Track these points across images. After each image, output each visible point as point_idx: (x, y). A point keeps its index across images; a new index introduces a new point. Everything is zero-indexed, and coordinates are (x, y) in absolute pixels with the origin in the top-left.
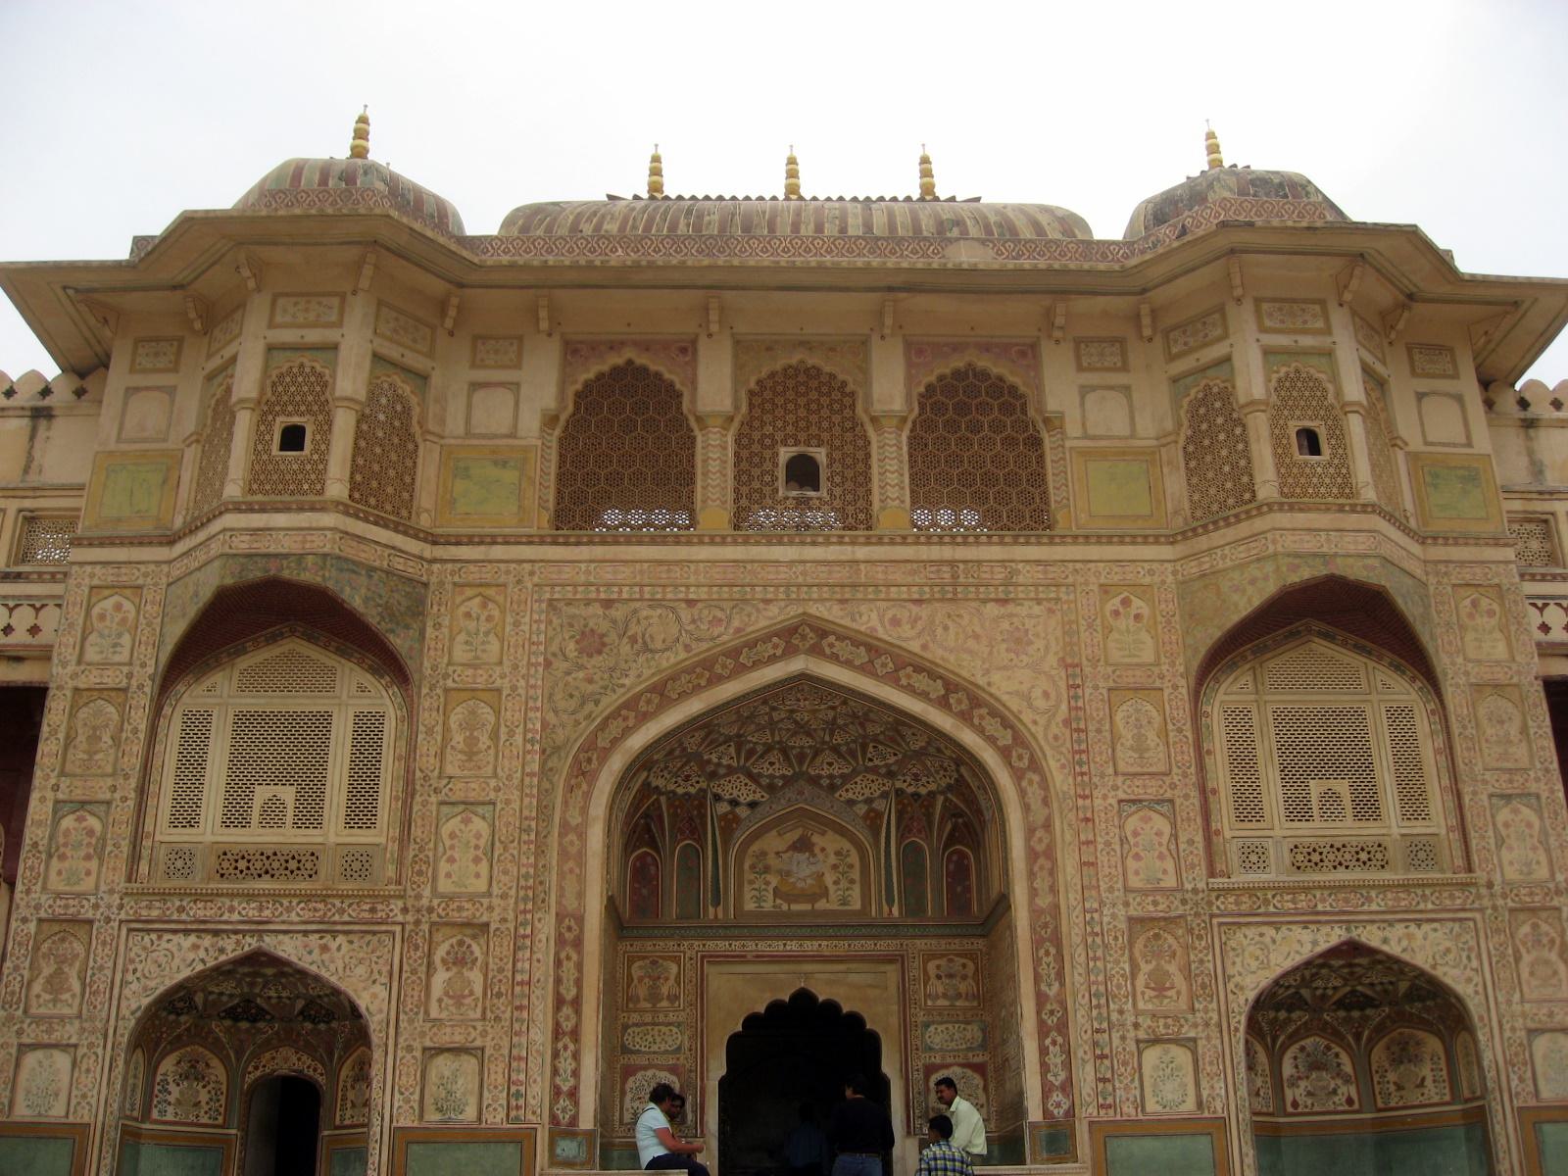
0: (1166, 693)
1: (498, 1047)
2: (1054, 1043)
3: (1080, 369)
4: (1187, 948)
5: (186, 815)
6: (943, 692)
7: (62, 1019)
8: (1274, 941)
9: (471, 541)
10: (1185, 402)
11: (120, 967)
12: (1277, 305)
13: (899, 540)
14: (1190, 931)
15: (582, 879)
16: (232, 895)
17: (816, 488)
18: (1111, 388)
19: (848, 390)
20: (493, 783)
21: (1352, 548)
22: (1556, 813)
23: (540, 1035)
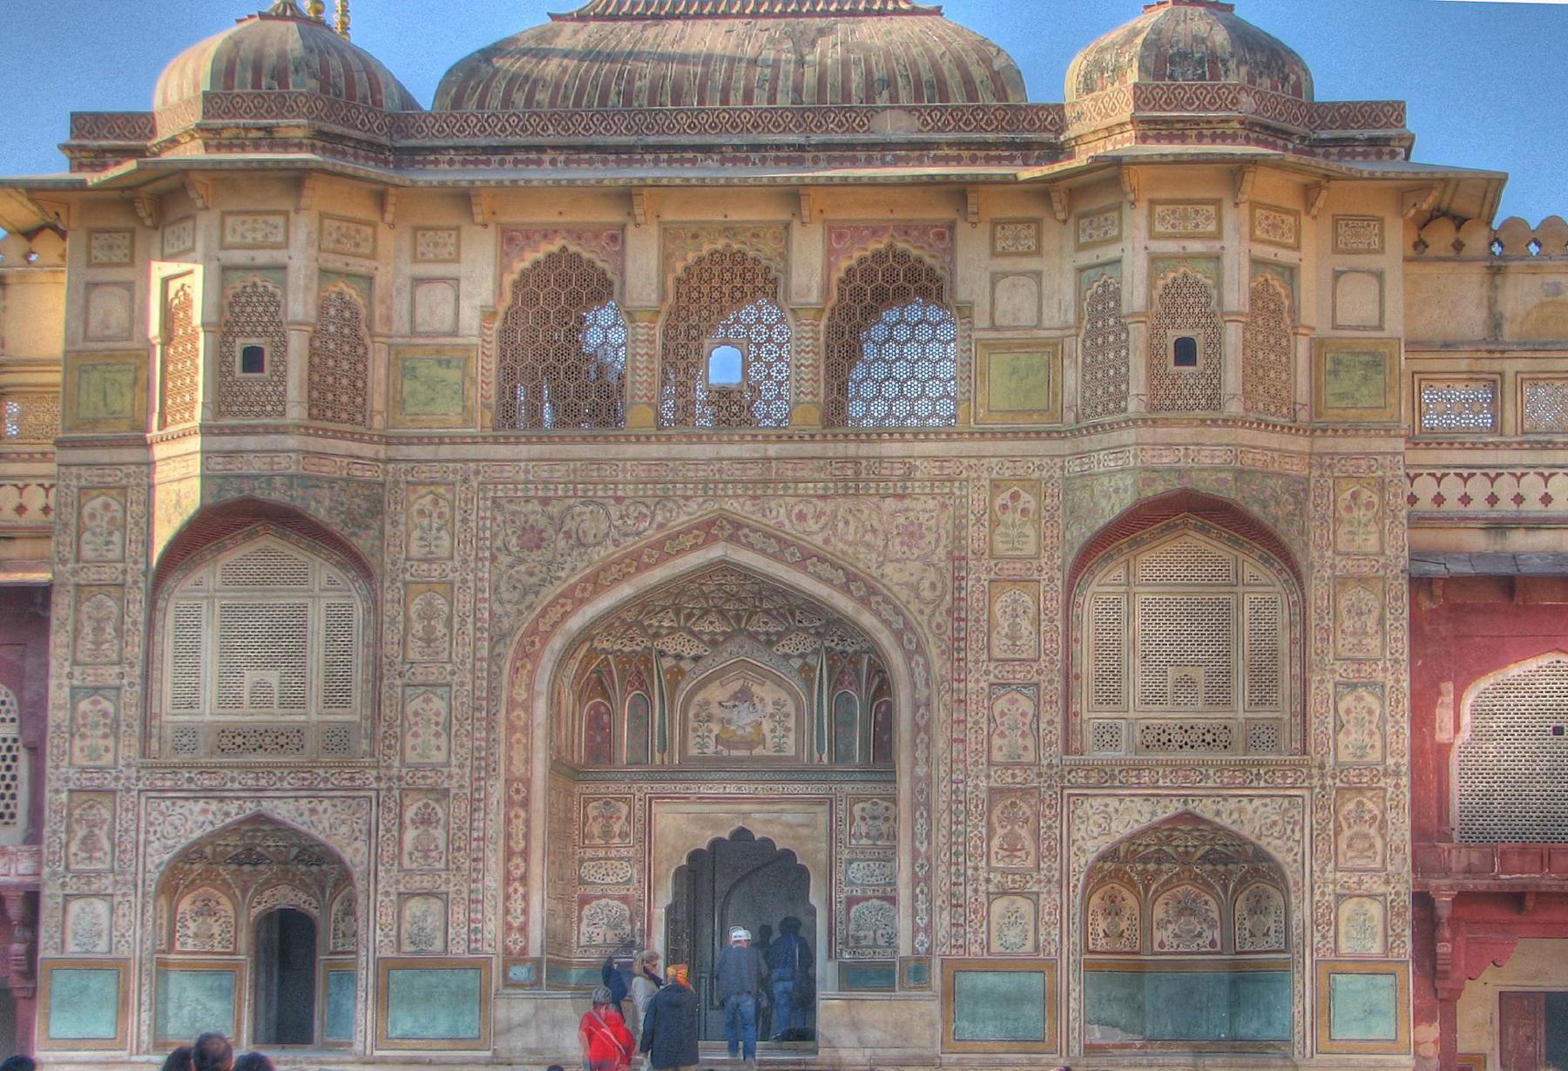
4: (1038, 815)
7: (98, 874)
9: (420, 440)
11: (142, 830)
15: (529, 749)
19: (771, 277)
20: (449, 667)
22: (1398, 701)
23: (493, 880)
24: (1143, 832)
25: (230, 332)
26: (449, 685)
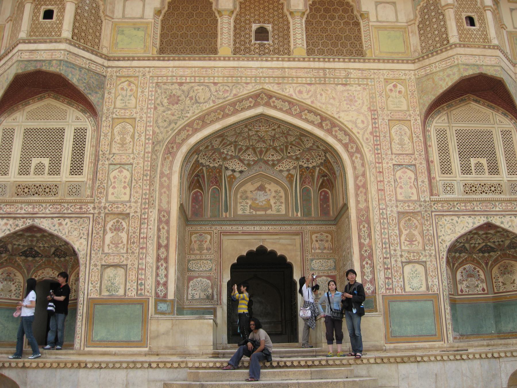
0: (412, 122)
1: (133, 265)
2: (367, 263)
6: (320, 121)
8: (457, 222)
9: (124, 59)
10: (419, 8)
13: (302, 59)
14: (423, 218)
15: (169, 196)
16: (22, 203)
17: (268, 40)
20: (132, 156)
21: (489, 63)
23: (151, 259)
26: (132, 164)
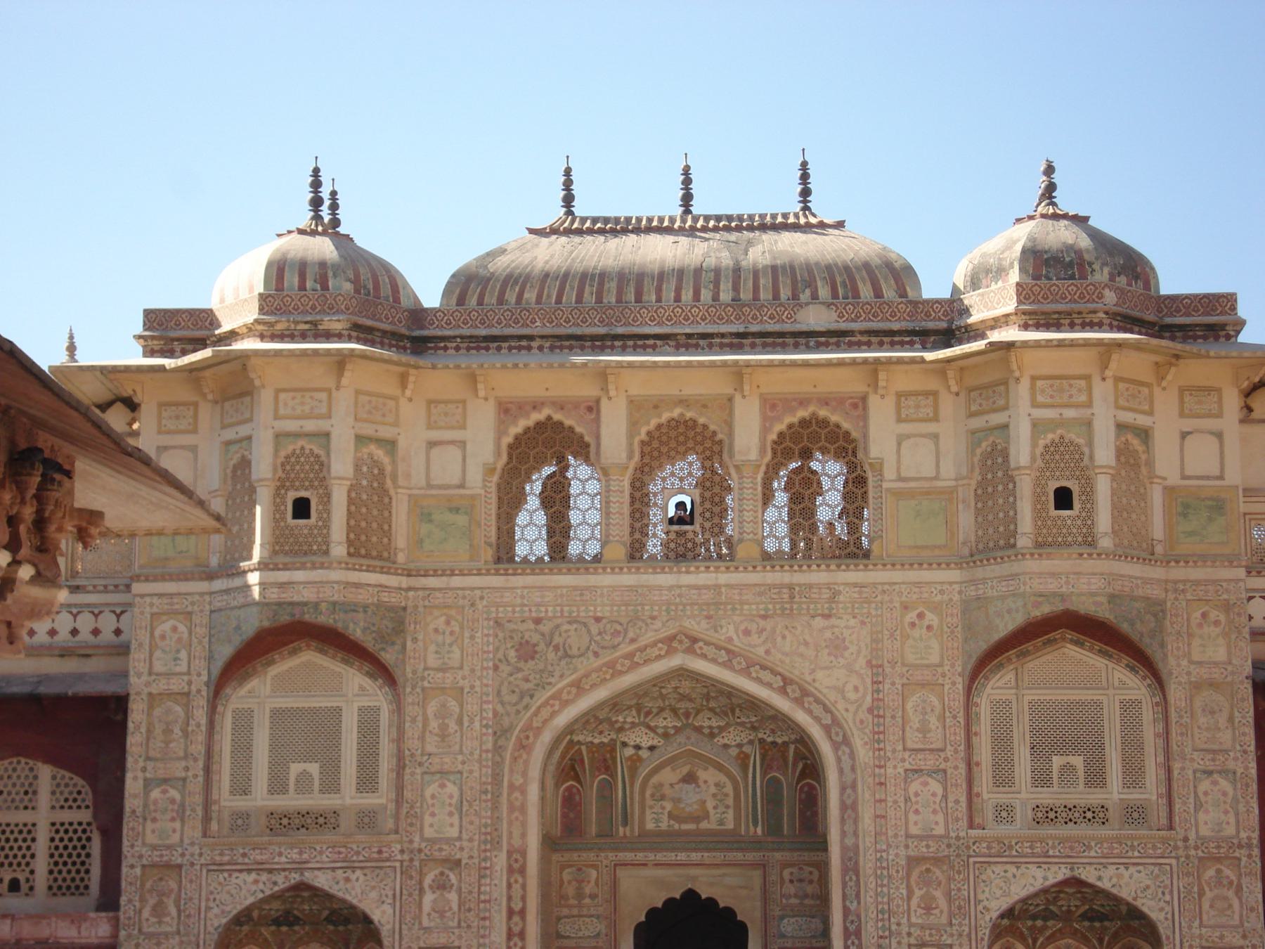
0: (947, 687)
3: (899, 420)
4: (949, 879)
5: (242, 787)
7: (167, 935)
8: (1014, 876)
9: (435, 574)
10: (978, 451)
12: (1049, 382)
15: (524, 824)
16: (280, 845)
18: (923, 436)
20: (460, 758)
22: (1247, 785)
24: (1036, 895)
25: (283, 486)
26: (460, 772)
